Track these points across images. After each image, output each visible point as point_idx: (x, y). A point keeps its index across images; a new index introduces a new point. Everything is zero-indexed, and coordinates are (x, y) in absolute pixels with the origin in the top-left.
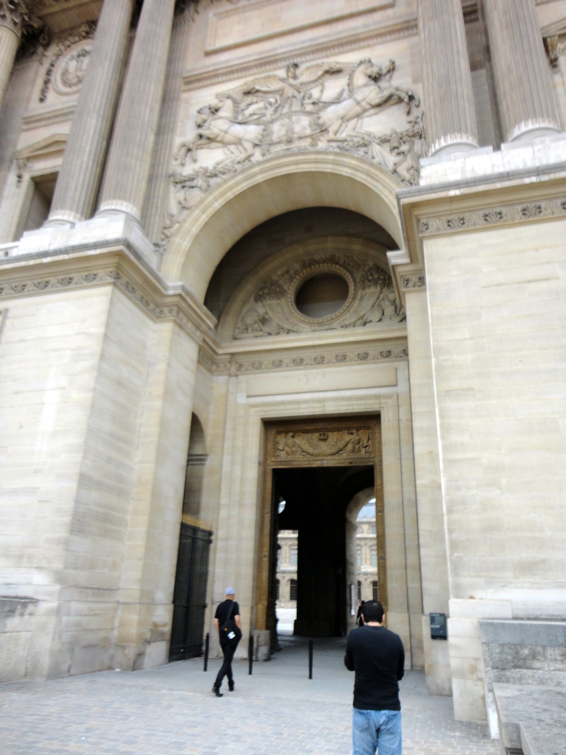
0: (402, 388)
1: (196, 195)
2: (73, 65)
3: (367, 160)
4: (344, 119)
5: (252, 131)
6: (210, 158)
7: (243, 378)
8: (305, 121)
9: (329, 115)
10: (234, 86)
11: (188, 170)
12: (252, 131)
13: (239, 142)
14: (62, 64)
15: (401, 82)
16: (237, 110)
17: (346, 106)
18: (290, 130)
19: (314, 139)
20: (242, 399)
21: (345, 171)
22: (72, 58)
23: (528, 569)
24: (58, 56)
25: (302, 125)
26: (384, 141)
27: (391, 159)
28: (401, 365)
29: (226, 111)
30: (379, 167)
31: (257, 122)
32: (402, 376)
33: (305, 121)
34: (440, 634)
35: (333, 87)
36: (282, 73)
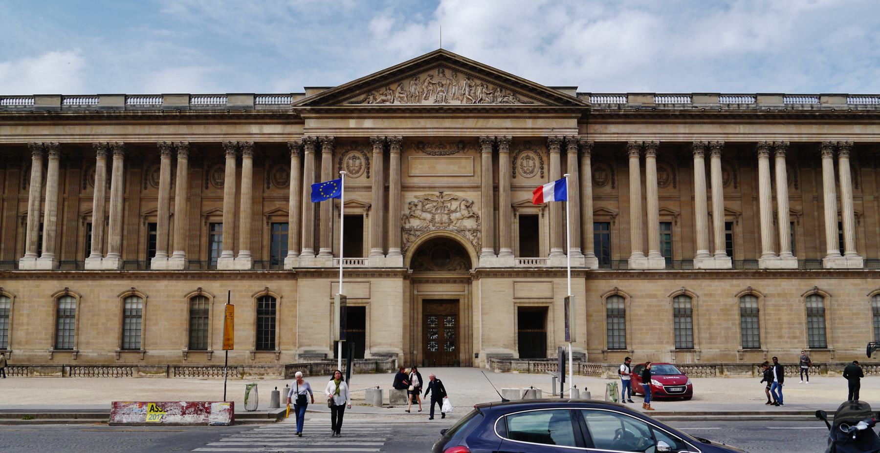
0: (466, 292)
1: (412, 238)
2: (351, 162)
3: (464, 236)
4: (458, 219)
5: (428, 216)
6: (415, 223)
7: (416, 285)
8: (446, 217)
9: (453, 216)
10: (420, 194)
11: (407, 226)
12: (428, 216)
13: (425, 219)
14: (346, 159)
15: (475, 209)
16: (423, 206)
17: (458, 215)
18: (441, 220)
19: (449, 225)
20: (416, 293)
21: (458, 239)
22: (350, 158)
23: (494, 345)
24: (343, 155)
25: (445, 218)
26: (469, 231)
27: (472, 238)
28: (466, 285)
29: (419, 207)
30: (468, 239)
31: (430, 212)
32: (466, 289)
33: (446, 217)
34: (477, 356)
35: (454, 205)
36: (437, 194)
